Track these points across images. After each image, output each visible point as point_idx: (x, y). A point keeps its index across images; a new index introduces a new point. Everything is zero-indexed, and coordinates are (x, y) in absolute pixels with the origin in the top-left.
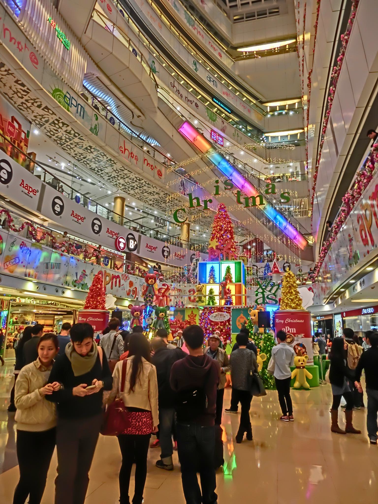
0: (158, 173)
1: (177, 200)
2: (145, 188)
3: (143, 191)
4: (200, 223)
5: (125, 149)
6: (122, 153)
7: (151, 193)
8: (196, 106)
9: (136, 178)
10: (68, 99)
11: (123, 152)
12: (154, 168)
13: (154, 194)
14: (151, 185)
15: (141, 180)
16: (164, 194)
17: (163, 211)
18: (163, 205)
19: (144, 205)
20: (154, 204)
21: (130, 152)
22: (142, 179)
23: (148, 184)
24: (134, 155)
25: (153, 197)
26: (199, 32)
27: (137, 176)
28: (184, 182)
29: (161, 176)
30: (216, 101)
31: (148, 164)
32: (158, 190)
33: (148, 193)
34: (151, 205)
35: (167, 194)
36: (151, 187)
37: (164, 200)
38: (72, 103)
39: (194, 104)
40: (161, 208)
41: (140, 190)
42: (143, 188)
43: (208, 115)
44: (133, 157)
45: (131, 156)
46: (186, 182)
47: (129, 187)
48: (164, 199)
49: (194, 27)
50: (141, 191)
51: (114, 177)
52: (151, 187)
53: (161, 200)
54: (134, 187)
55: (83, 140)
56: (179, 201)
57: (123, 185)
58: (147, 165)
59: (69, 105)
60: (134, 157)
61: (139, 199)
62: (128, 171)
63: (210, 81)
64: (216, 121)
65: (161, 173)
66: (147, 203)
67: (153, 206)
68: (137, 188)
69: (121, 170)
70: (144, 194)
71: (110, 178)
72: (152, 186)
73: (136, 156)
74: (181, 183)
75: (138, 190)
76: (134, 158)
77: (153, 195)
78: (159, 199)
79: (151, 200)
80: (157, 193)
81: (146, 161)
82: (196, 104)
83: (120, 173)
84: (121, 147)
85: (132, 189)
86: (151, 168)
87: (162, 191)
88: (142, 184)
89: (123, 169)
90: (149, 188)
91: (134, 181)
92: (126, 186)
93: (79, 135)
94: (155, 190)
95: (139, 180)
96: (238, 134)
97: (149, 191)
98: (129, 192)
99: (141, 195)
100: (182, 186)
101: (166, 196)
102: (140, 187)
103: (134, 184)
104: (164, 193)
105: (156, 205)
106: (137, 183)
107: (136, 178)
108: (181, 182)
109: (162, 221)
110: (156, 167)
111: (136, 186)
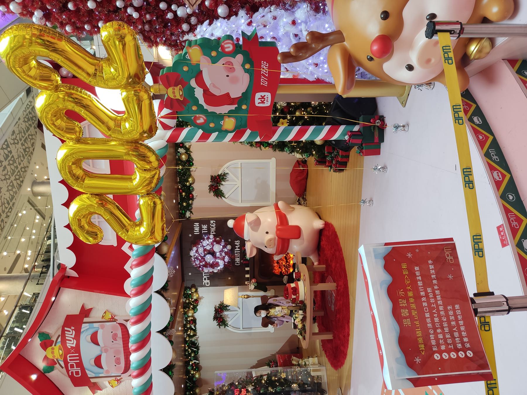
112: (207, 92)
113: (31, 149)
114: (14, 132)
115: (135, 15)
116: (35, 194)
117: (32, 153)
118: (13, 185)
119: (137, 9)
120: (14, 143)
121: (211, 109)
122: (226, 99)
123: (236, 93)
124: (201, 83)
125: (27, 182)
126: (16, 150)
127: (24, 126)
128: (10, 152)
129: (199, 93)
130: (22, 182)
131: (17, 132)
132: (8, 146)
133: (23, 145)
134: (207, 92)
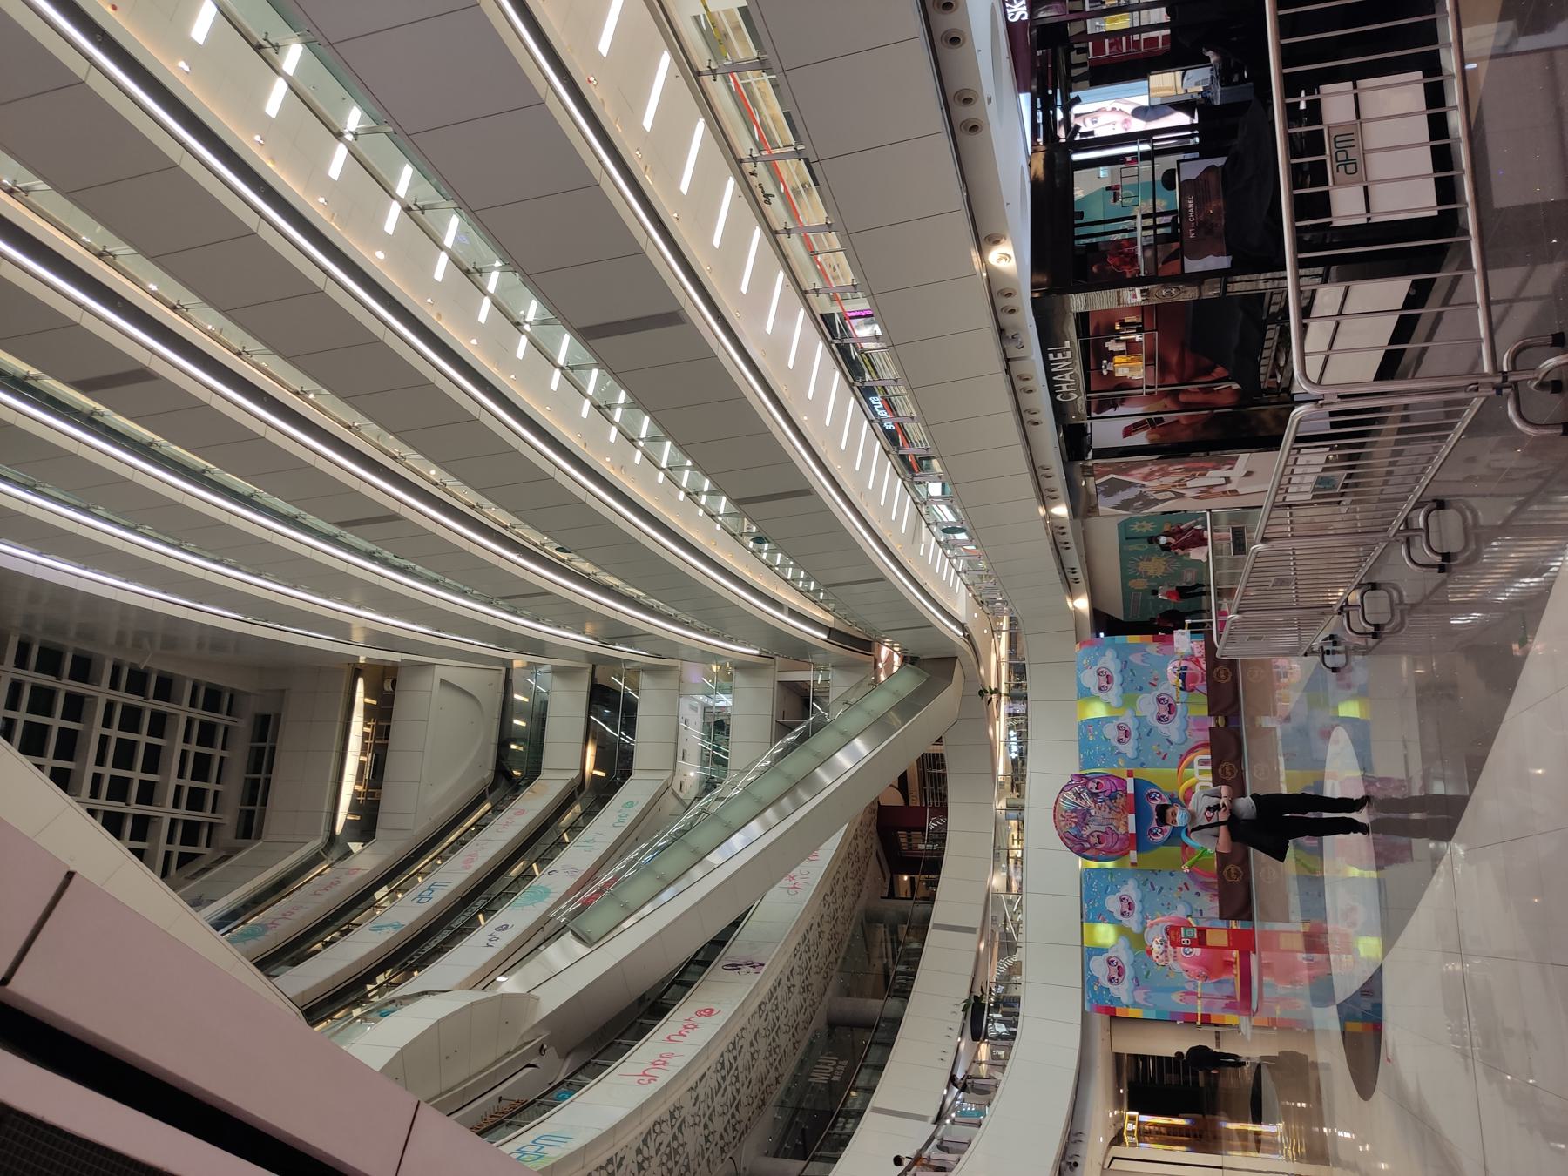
0: (706, 1016)
2: (740, 1062)
5: (644, 1075)
6: (655, 1080)
8: (506, 929)
10: (525, 1156)
11: (653, 1079)
16: (760, 1017)
21: (652, 1066)
25: (762, 1055)
26: (284, 915)
27: (713, 1069)
28: (730, 963)
29: (712, 1010)
30: (440, 938)
35: (760, 1006)
37: (773, 1030)
38: (536, 1152)
39: (498, 934)
43: (533, 904)
44: (665, 1062)
45: (662, 1064)
47: (733, 1116)
49: (270, 926)
50: (747, 1083)
51: (707, 1140)
55: (622, 1158)
56: (779, 984)
57: (725, 1130)
58: (685, 1036)
59: (541, 1157)
60: (663, 1059)
62: (701, 1080)
63: (430, 897)
64: (549, 887)
65: (704, 1011)
69: (694, 1105)
71: (706, 1156)
73: (661, 1056)
74: (733, 970)
76: (668, 1060)
81: (672, 1038)
82: (498, 929)
83: (701, 1113)
84: (638, 1082)
89: (694, 1094)
92: (729, 1122)
93: (610, 1161)
94: (750, 1037)
98: (743, 1125)
101: (764, 1014)
104: (757, 1016)
110: (689, 1020)
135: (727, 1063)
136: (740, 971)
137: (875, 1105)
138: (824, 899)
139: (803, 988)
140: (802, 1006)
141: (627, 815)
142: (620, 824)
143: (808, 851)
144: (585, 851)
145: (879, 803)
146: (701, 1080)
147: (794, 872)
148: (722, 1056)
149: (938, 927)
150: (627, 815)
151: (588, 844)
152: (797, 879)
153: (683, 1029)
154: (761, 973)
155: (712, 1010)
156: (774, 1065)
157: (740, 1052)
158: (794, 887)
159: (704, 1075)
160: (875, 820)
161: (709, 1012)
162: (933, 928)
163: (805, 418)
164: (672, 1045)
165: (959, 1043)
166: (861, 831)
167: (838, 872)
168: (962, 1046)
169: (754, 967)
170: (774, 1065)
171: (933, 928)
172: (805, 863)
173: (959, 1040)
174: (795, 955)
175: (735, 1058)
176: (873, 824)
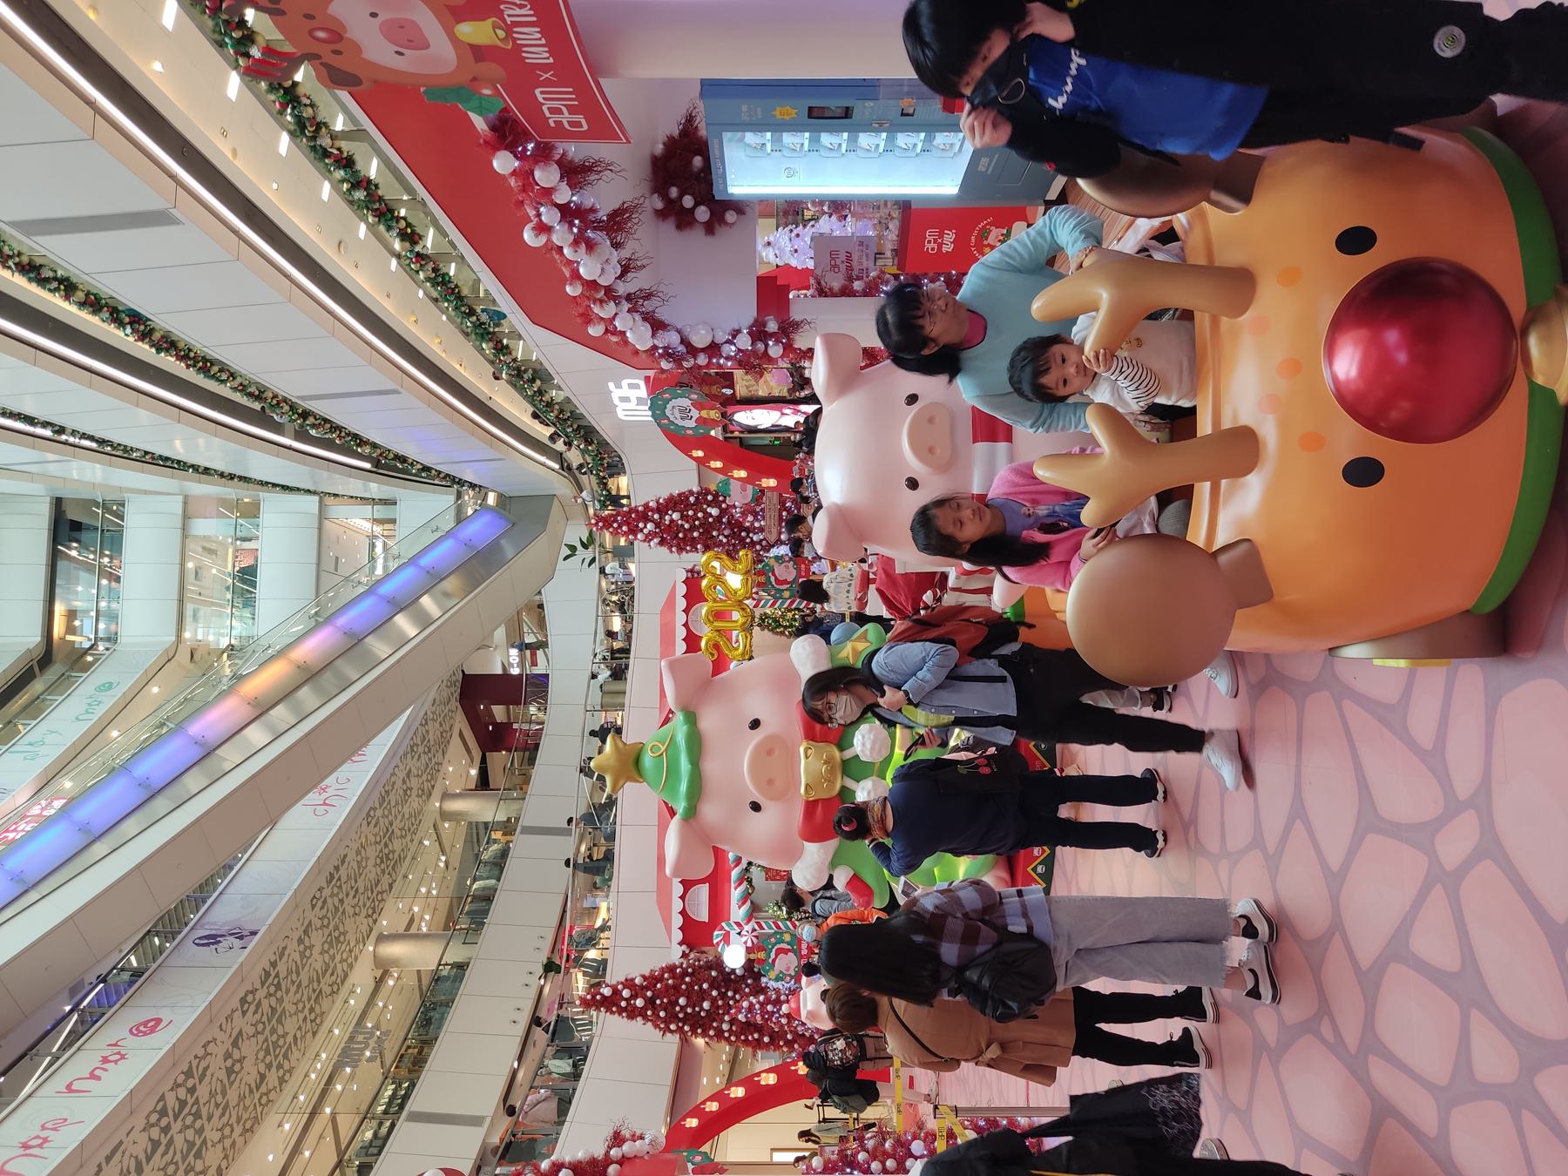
0: (145, 1034)
1: (274, 964)
2: (203, 1092)
3: (217, 1105)
4: (382, 893)
7: (230, 1071)
9: (150, 1126)
12: (116, 1049)
13: (236, 1055)
14: (195, 1063)
15: (165, 1107)
16: (244, 1013)
17: (314, 1034)
18: (291, 1025)
19: (283, 1109)
20: (280, 1066)
21: (21, 1151)
22: (162, 1098)
23: (189, 1074)
24: (37, 1137)
25: (248, 1064)
27: (140, 1122)
28: (208, 933)
29: (159, 1021)
31: (93, 1076)
32: (220, 1036)
33: (231, 1084)
34: (282, 1081)
35: (243, 1001)
36: (203, 1064)
37: (269, 1021)
40: (303, 1037)
41: (210, 1118)
42: (202, 1102)
44: (45, 1140)
45: (40, 1146)
46: (202, 927)
48: (265, 1019)
50: (217, 1113)
52: (203, 1064)
53: (267, 1032)
54: (191, 1144)
56: (282, 955)
58: (98, 1078)
60: (44, 1134)
61: (251, 1130)
62: (108, 1159)
65: (145, 1024)
66: (272, 1096)
67: (291, 1071)
68: (200, 1131)
70: (232, 1104)
72: (201, 1059)
73: (43, 1128)
75: (207, 1127)
77: (241, 1060)
78: (261, 1038)
79: (263, 1077)
80: (235, 1044)
85: (198, 1156)
86: (116, 1062)
87: (229, 1018)
88: (183, 1104)
90: (208, 1073)
91: (164, 1141)
94: (218, 1050)
95: (163, 1113)
96: (31, 744)
97: (222, 1075)
99: (233, 1120)
100: (220, 942)
101: (253, 1008)
102: (197, 1116)
103: (179, 1141)
104: (239, 1013)
105: (286, 1057)
106: (176, 1127)
107: (150, 1126)
108: (198, 945)
109: (360, 1038)
110: (116, 1045)
111: (190, 1134)
112: (776, 578)
113: (449, 734)
114: (434, 701)
115: (725, 540)
116: (445, 815)
117: (448, 742)
118: (423, 791)
119: (726, 537)
120: (433, 719)
121: (778, 587)
122: (785, 582)
123: (790, 579)
124: (774, 574)
125: (437, 793)
126: (434, 730)
127: (446, 692)
128: (427, 731)
129: (773, 579)
130: (433, 787)
131: (438, 702)
132: (427, 723)
133: (441, 725)
134: (776, 578)
135: (171, 1102)
136: (219, 947)
137: (412, 1109)
138: (368, 815)
139: (331, 944)
140: (327, 965)
141: (100, 702)
142: (89, 716)
143: (351, 749)
144: (25, 759)
145: (463, 671)
146: (108, 1159)
147: (328, 781)
148: (162, 1098)
149: (529, 830)
150: (100, 702)
151: (29, 748)
152: (331, 791)
153: (99, 1065)
154: (247, 951)
155: (159, 1021)
156: (275, 1064)
157: (203, 1076)
158: (325, 804)
159: (121, 1143)
160: (457, 695)
161: (152, 1026)
162: (521, 833)
163: (157, 66)
164: (71, 1101)
165: (542, 988)
166: (433, 713)
167: (393, 774)
168: (547, 990)
169: (241, 938)
170: (275, 1064)
171: (521, 833)
172: (347, 766)
173: (542, 981)
174: (313, 907)
175: (192, 1091)
176: (453, 700)
